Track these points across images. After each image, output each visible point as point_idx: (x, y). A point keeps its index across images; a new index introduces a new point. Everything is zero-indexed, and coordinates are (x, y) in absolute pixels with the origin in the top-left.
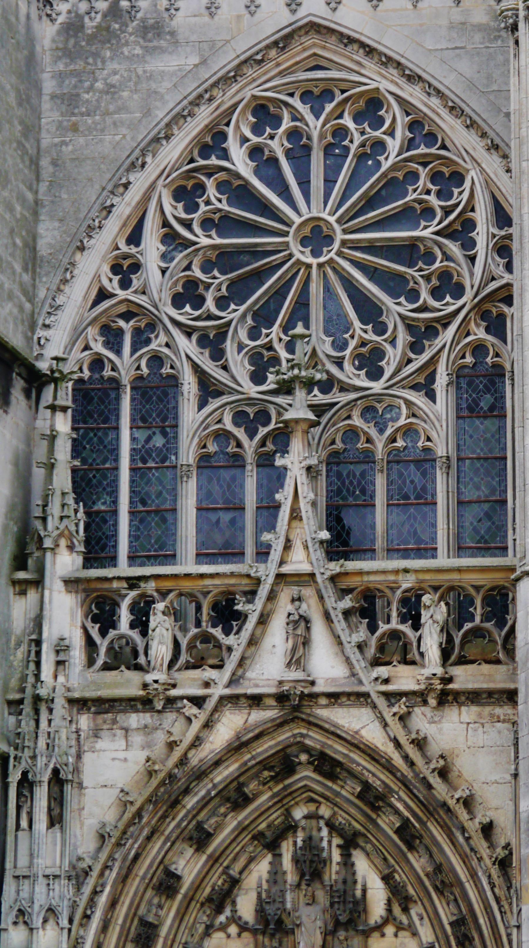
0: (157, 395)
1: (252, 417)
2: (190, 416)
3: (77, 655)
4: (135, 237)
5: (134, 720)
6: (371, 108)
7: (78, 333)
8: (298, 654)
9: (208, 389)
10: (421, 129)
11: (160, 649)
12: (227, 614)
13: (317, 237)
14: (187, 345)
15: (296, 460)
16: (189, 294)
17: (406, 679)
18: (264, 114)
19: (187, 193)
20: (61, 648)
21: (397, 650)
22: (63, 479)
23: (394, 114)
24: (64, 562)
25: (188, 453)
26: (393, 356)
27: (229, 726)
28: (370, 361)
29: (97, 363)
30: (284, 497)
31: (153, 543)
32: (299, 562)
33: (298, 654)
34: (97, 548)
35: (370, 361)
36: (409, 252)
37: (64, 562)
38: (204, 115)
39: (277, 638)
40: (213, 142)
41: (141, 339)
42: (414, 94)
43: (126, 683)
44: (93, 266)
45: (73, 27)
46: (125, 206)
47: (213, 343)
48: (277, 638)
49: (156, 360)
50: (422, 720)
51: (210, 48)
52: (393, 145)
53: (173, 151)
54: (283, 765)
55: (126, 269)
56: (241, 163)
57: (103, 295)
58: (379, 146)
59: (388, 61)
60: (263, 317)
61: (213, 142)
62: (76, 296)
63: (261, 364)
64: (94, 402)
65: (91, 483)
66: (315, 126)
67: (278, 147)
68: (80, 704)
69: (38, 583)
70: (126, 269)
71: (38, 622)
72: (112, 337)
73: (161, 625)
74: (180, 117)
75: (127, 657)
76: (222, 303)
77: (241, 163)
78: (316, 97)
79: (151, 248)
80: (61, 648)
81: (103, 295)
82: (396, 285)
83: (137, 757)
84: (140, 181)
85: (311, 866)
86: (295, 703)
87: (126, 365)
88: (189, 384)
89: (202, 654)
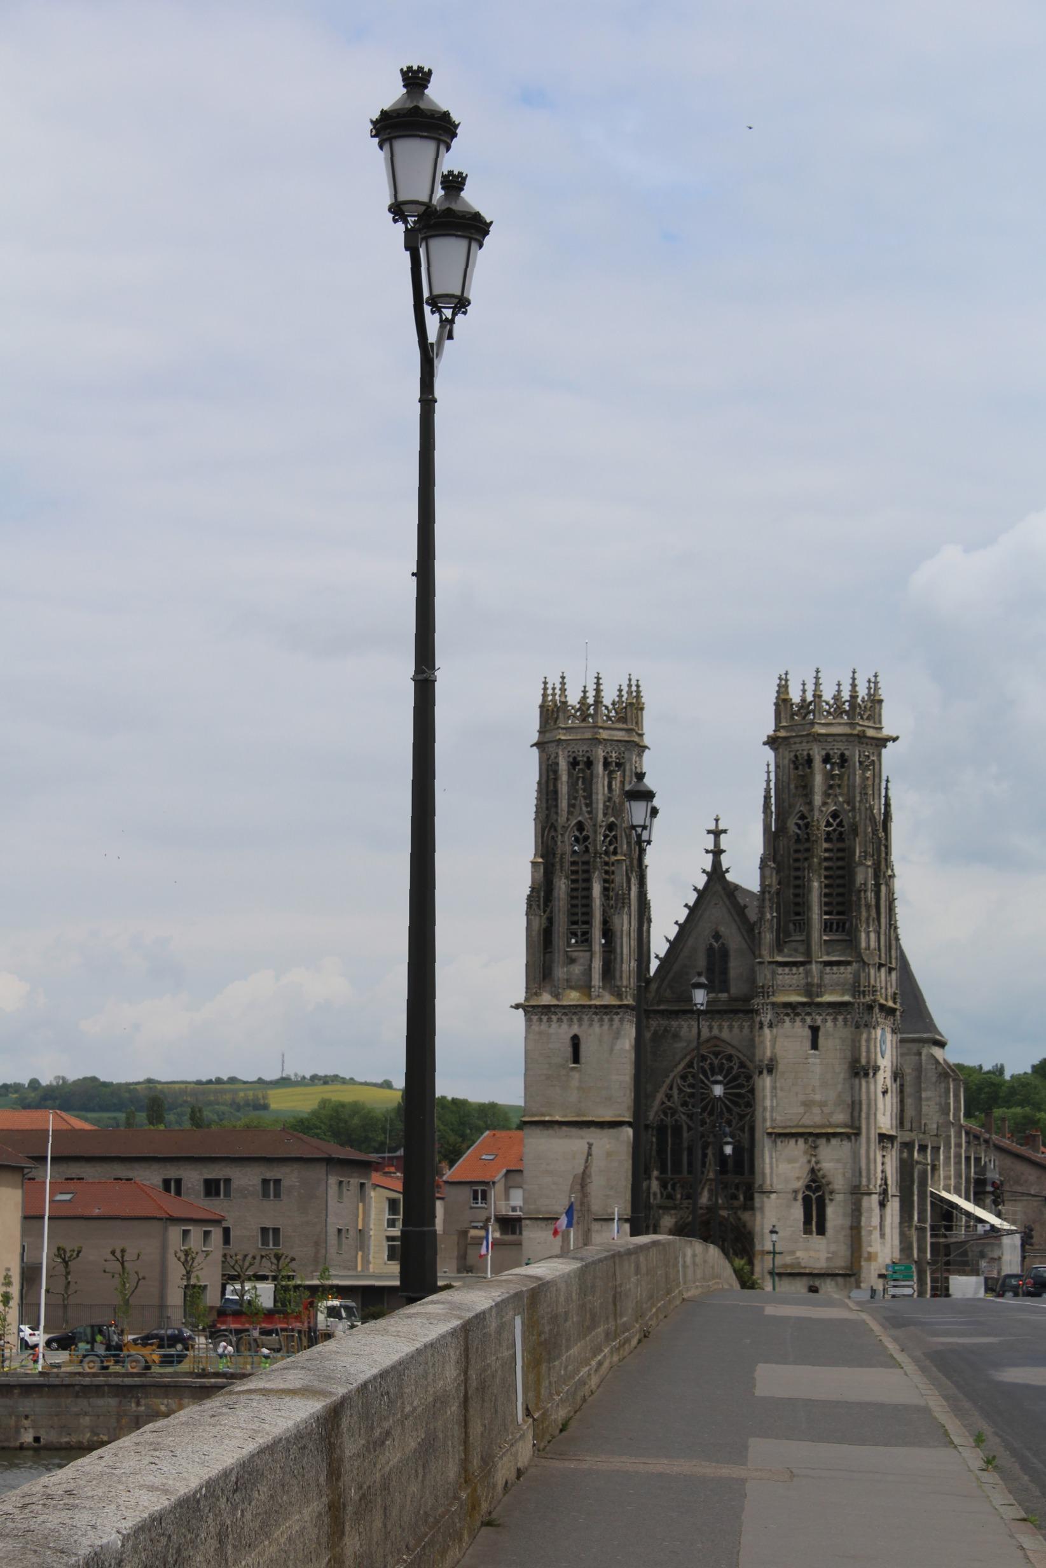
0: (677, 1129)
2: (685, 1135)
3: (659, 1196)
4: (671, 1088)
5: (673, 1212)
6: (730, 1058)
7: (657, 1113)
9: (690, 1129)
10: (742, 1065)
11: (679, 1196)
14: (684, 1117)
16: (685, 1104)
17: (736, 1203)
18: (703, 1058)
19: (684, 1078)
20: (655, 1194)
21: (735, 1197)
22: (654, 1153)
23: (735, 1060)
24: (655, 1173)
25: (685, 1145)
26: (734, 1122)
29: (662, 1120)
30: (707, 1160)
31: (677, 1169)
34: (663, 1170)
36: (739, 1095)
37: (655, 1173)
38: (688, 1058)
41: (673, 1115)
42: (740, 1056)
43: (670, 1203)
44: (660, 1096)
45: (655, 1033)
46: (668, 1081)
49: (676, 1121)
50: (739, 1213)
52: (736, 1067)
53: (681, 1067)
55: (669, 1097)
57: (663, 1103)
58: (732, 1068)
59: (733, 1047)
61: (690, 1065)
62: (657, 1103)
65: (661, 1151)
66: (716, 1062)
67: (707, 1067)
68: (660, 1207)
69: (649, 1178)
70: (669, 1097)
71: (649, 1188)
72: (665, 1114)
73: (679, 1190)
74: (682, 1059)
76: (693, 1106)
78: (716, 1054)
79: (675, 1092)
80: (655, 1194)
81: (663, 1103)
82: (736, 1104)
83: (674, 1220)
84: (672, 1075)
87: (669, 1121)
88: (685, 1128)
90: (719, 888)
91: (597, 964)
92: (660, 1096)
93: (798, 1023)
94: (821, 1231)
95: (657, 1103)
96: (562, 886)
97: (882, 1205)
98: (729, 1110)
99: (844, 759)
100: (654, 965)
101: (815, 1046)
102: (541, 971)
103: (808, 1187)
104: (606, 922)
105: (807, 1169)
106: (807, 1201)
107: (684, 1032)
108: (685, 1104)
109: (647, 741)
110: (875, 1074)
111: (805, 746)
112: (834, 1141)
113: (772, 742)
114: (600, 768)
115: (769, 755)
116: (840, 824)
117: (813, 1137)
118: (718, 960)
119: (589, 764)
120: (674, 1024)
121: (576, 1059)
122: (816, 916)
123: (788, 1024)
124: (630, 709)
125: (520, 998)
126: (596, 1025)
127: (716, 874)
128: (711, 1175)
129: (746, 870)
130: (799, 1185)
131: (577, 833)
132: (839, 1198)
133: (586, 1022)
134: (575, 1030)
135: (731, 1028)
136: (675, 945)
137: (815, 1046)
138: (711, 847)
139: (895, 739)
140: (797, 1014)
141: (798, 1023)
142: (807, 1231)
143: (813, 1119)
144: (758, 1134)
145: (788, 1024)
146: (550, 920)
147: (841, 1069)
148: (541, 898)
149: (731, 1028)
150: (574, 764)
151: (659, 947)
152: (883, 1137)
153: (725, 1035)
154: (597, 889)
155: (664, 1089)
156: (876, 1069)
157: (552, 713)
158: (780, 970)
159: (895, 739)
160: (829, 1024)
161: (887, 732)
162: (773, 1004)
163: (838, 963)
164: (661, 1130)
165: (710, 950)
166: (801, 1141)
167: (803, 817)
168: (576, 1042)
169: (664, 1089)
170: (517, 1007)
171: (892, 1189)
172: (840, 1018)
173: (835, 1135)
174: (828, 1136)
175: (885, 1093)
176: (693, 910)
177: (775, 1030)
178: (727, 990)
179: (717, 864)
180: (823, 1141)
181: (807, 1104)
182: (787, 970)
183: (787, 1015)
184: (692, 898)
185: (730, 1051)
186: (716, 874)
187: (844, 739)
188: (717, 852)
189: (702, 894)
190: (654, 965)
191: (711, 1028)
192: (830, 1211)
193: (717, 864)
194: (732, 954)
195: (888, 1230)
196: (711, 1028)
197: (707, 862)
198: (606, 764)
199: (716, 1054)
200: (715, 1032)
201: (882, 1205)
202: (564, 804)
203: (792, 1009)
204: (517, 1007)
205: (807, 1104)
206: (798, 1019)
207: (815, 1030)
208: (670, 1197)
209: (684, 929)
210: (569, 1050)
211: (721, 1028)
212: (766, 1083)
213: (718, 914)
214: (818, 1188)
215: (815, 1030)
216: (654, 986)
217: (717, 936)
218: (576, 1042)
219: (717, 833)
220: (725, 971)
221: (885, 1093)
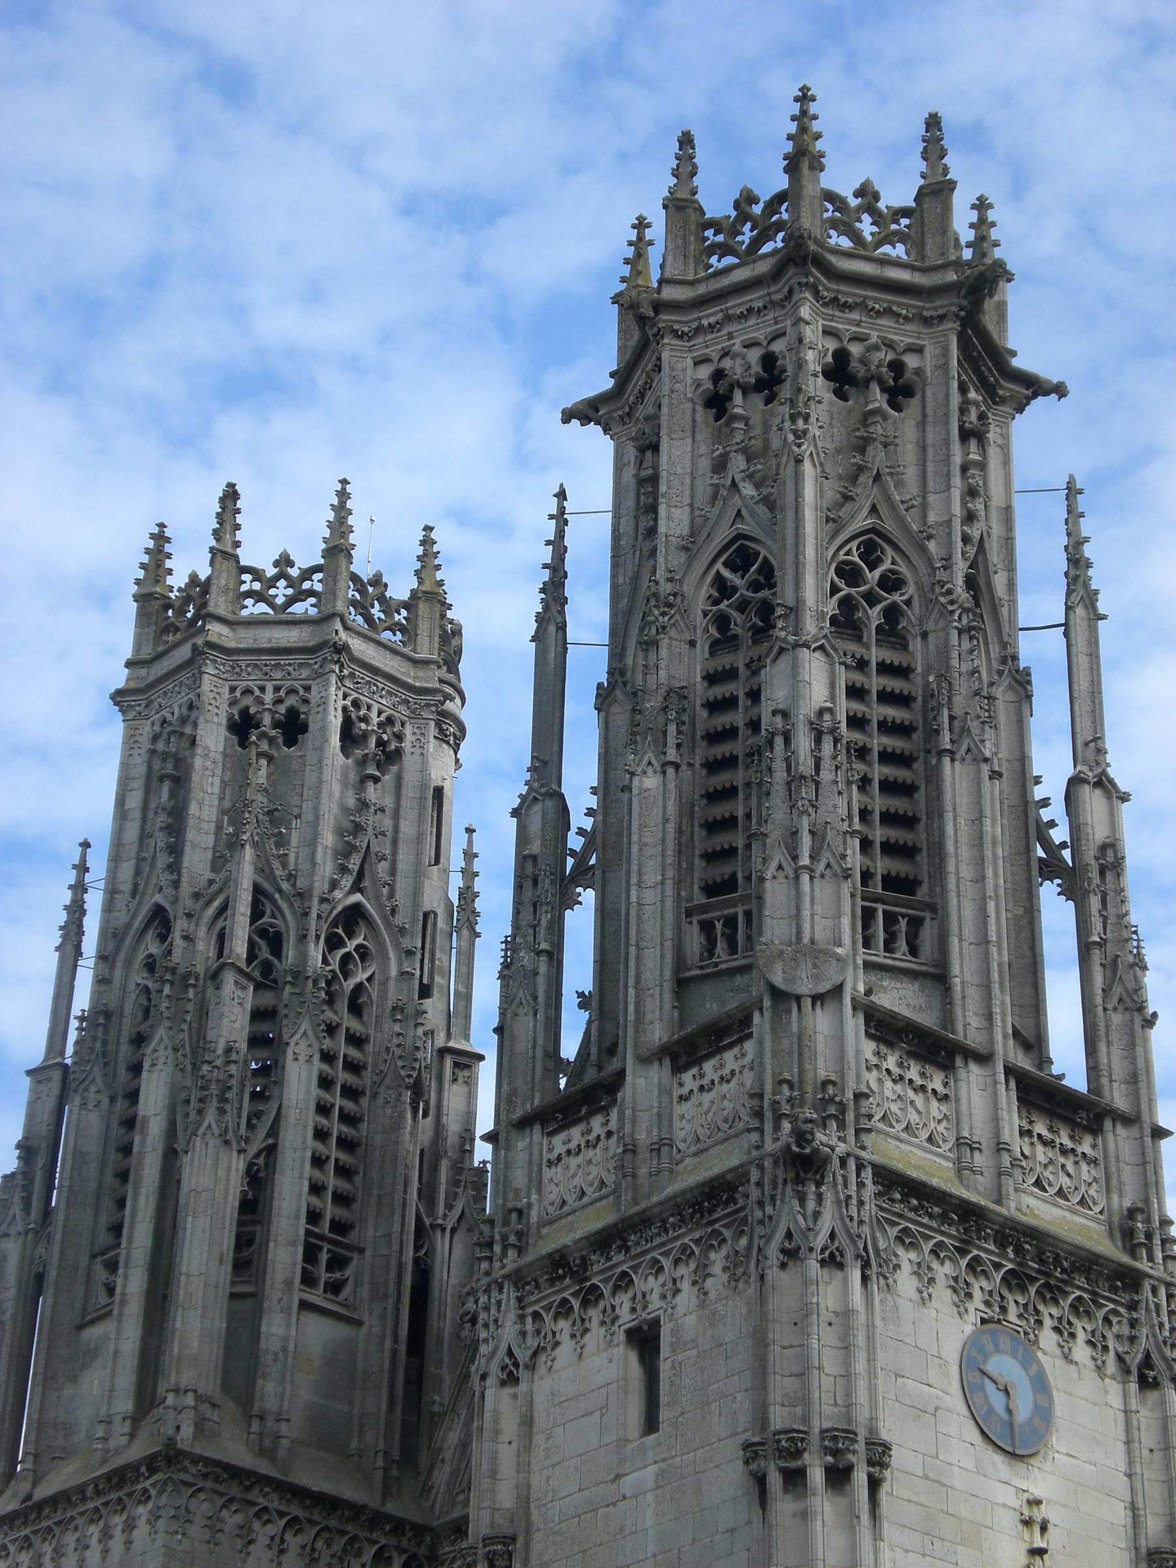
93: (596, 1334)
110: (838, 1477)
123: (565, 1350)
131: (154, 949)
140: (590, 1296)
147: (726, 1477)
158: (558, 1144)
160: (686, 1298)
162: (518, 1278)
172: (718, 1259)
177: (523, 1387)
182: (575, 1134)
183: (564, 1309)
187: (755, 298)
198: (242, 727)
203: (572, 1277)
206: (594, 1314)
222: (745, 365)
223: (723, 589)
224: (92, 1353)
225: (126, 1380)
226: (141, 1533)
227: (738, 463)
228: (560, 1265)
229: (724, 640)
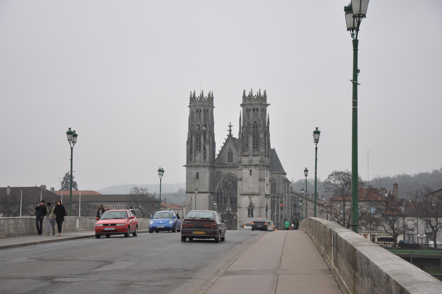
0: (221, 194)
1: (227, 195)
6: (233, 177)
8: (229, 209)
12: (225, 207)
13: (230, 185)
15: (228, 199)
16: (223, 188)
17: (234, 210)
18: (227, 177)
19: (223, 182)
27: (225, 213)
28: (233, 192)
32: (229, 204)
33: (229, 209)
35: (233, 192)
39: (228, 208)
40: (224, 179)
43: (220, 210)
44: (218, 186)
47: (224, 191)
48: (228, 208)
51: (224, 174)
54: (228, 215)
55: (220, 186)
56: (226, 180)
60: (227, 189)
61: (224, 179)
62: (217, 188)
63: (227, 192)
64: (218, 194)
70: (220, 186)
75: (220, 209)
77: (226, 180)
78: (230, 176)
79: (221, 185)
85: (230, 220)
86: (229, 211)
89: (224, 209)
90: (230, 139)
91: (203, 156)
92: (218, 186)
93: (247, 169)
94: (252, 216)
95: (217, 188)
96: (194, 139)
97: (267, 210)
98: (233, 189)
99: (257, 110)
100: (216, 156)
101: (251, 175)
102: (189, 158)
103: (249, 207)
104: (204, 146)
105: (249, 202)
106: (249, 210)
107: (223, 172)
108: (223, 188)
109: (214, 105)
111: (249, 106)
112: (255, 196)
113: (242, 105)
114: (202, 112)
115: (241, 109)
116: (257, 124)
117: (250, 195)
118: (230, 155)
119: (201, 111)
120: (221, 170)
121: (198, 178)
122: (251, 145)
123: (245, 170)
124: (211, 99)
125: (185, 164)
126: (202, 170)
127: (230, 136)
128: (229, 204)
129: (236, 135)
130: (248, 206)
132: (256, 209)
133: (200, 170)
134: (197, 171)
135: (233, 171)
136: (221, 152)
137: (251, 175)
138: (229, 129)
139: (269, 105)
141: (247, 169)
142: (249, 217)
143: (250, 191)
144: (238, 195)
145: (245, 170)
146: (192, 146)
147: (257, 179)
148: (189, 142)
149: (233, 171)
150: (197, 111)
151: (217, 152)
152: (266, 195)
153: (232, 172)
154: (202, 139)
155: (218, 185)
156: (265, 180)
157: (193, 99)
159: (269, 105)
160: (254, 169)
161: (267, 103)
163: (256, 156)
164: (218, 194)
165: (229, 153)
166: (248, 196)
167: (248, 123)
168: (198, 174)
169: (218, 185)
170: (184, 166)
171: (269, 207)
173: (255, 195)
174: (254, 195)
175: (267, 185)
176: (225, 144)
178: (232, 162)
179: (230, 133)
180: (252, 196)
181: (249, 188)
184: (225, 141)
185: (233, 176)
186: (230, 136)
188: (230, 131)
189: (227, 140)
190: (216, 156)
191: (229, 171)
192: (254, 212)
193: (230, 133)
194: (234, 154)
195: (268, 216)
196: (229, 171)
197: (228, 133)
198: (204, 111)
199: (230, 176)
200: (230, 171)
201: (267, 210)
202: (195, 120)
203: (246, 166)
204: (184, 166)
205: (249, 188)
207: (251, 171)
208: (220, 209)
209: (223, 148)
210: (196, 176)
211: (231, 171)
212: (239, 183)
213: (231, 145)
214: (252, 207)
215: (251, 171)
216: (216, 161)
217: (230, 150)
218: (198, 174)
219: (230, 126)
220: (232, 158)
221: (267, 185)
222: (256, 108)
223: (254, 124)
224: (197, 156)
225: (202, 159)
226: (207, 169)
227: (256, 116)
228: (245, 165)
229: (254, 127)
